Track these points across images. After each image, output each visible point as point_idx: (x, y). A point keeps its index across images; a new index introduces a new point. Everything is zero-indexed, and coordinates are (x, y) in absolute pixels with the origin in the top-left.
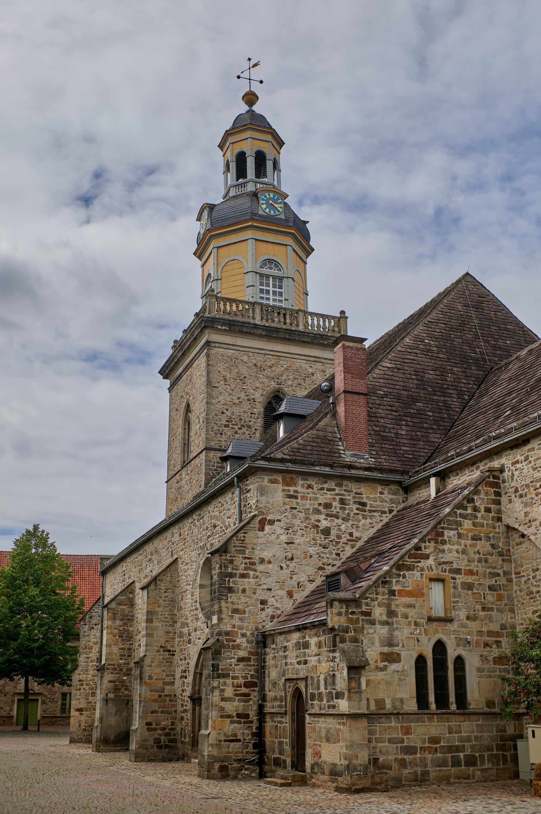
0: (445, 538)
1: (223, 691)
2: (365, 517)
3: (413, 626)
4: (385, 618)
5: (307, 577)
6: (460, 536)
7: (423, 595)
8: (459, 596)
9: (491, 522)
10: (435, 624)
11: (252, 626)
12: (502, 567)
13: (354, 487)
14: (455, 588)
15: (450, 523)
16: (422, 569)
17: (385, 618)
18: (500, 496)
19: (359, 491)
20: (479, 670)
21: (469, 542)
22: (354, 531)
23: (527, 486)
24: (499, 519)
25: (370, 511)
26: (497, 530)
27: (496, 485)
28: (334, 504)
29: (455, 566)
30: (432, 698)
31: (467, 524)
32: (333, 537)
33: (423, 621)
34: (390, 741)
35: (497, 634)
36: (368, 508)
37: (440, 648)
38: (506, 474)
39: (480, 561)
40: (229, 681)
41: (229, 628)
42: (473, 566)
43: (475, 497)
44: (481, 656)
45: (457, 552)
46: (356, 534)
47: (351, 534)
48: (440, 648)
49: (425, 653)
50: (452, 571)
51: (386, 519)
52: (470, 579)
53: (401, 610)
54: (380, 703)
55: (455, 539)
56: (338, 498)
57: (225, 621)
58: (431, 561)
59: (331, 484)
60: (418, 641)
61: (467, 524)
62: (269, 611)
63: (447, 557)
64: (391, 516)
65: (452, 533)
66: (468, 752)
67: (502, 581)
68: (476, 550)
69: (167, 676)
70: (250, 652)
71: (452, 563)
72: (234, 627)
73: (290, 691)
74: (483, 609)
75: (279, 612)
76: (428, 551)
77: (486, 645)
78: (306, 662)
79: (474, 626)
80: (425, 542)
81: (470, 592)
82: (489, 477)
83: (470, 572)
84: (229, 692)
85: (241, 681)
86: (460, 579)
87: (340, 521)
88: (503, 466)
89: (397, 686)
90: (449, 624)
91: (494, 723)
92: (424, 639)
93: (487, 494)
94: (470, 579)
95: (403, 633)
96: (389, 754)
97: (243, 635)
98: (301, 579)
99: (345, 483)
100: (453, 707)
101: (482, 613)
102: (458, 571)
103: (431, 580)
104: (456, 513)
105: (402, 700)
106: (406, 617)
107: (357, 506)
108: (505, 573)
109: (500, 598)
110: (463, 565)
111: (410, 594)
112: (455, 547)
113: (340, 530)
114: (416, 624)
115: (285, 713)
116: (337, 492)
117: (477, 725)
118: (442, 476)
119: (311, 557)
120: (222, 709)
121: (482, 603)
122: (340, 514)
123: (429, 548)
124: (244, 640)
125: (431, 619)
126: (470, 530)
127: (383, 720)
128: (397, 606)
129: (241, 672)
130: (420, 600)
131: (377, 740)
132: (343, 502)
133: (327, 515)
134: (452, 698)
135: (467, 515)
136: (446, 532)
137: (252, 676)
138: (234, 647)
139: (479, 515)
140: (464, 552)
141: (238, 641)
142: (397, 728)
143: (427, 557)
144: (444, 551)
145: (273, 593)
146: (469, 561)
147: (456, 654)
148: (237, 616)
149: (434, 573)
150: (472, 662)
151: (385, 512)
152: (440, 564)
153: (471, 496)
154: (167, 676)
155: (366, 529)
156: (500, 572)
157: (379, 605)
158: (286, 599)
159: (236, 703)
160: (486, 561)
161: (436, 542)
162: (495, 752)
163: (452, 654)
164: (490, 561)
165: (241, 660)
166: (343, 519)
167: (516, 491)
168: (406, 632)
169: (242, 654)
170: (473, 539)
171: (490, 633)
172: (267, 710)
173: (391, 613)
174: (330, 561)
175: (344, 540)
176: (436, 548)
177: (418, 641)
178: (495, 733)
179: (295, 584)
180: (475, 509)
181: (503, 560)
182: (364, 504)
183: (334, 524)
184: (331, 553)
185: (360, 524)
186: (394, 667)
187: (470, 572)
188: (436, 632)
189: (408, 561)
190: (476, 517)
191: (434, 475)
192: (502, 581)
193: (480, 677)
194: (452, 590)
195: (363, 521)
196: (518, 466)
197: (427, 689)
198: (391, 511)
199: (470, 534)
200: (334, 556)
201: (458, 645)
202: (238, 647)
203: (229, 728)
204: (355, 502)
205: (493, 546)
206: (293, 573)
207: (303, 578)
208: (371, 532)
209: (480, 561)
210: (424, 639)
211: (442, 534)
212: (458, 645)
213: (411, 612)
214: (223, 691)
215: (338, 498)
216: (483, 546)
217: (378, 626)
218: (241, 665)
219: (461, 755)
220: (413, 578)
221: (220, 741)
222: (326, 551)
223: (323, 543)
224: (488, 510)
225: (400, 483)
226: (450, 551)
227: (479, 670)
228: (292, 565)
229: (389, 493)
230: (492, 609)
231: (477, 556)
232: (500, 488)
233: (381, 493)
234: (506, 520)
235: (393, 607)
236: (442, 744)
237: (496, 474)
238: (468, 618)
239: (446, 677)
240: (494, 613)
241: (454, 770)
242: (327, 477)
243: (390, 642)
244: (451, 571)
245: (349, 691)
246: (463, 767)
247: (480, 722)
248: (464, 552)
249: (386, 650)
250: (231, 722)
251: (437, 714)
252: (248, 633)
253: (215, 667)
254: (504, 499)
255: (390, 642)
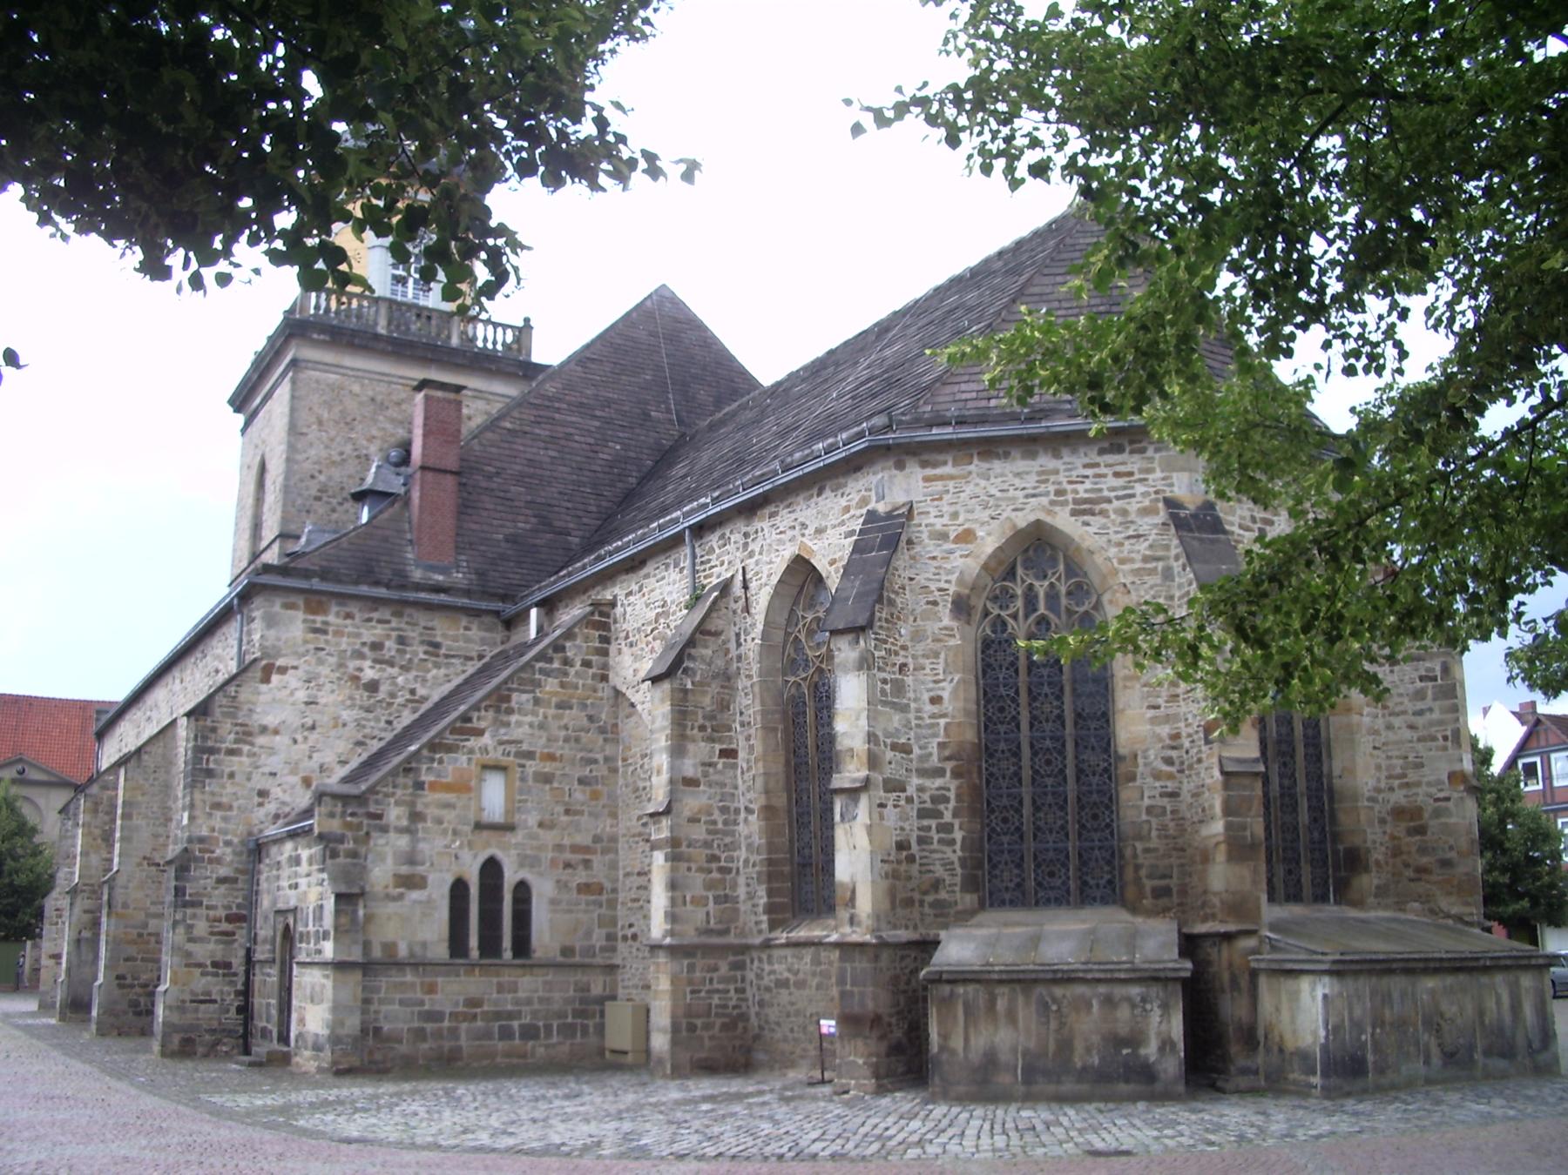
0: (513, 704)
1: (191, 927)
2: (437, 666)
3: (450, 837)
4: (405, 823)
5: (334, 757)
6: (537, 702)
7: (468, 789)
8: (529, 792)
9: (589, 681)
10: (485, 834)
11: (241, 829)
12: (603, 750)
13: (423, 619)
14: (523, 779)
15: (522, 682)
16: (471, 751)
17: (405, 823)
18: (609, 643)
19: (430, 624)
20: (553, 902)
21: (552, 711)
22: (417, 686)
23: (639, 630)
24: (604, 678)
25: (447, 656)
26: (600, 694)
27: (605, 626)
28: (387, 644)
29: (525, 747)
30: (474, 942)
31: (551, 685)
32: (381, 695)
33: (468, 829)
34: (401, 1002)
35: (586, 849)
36: (443, 651)
37: (491, 869)
38: (619, 610)
39: (566, 740)
40: (202, 912)
41: (205, 832)
42: (559, 749)
43: (568, 644)
44: (558, 882)
45: (531, 725)
46: (421, 691)
47: (413, 692)
48: (491, 869)
49: (467, 877)
50: (519, 754)
51: (471, 668)
52: (548, 767)
53: (432, 812)
54: (390, 948)
55: (530, 706)
56: (394, 634)
57: (200, 821)
58: (487, 739)
59: (385, 613)
60: (457, 857)
61: (551, 685)
62: (271, 807)
63: (517, 733)
64: (479, 664)
65: (525, 697)
66: (527, 1020)
67: (601, 770)
68: (562, 723)
69: (153, 903)
70: (237, 870)
71: (521, 742)
72: (213, 830)
73: (280, 927)
74: (567, 812)
75: (287, 809)
76: (483, 724)
77: (568, 865)
78: (296, 886)
79: (549, 837)
80: (479, 710)
81: (547, 787)
82: (592, 613)
83: (551, 757)
84: (201, 927)
85: (222, 913)
86: (532, 766)
87: (395, 671)
88: (615, 597)
89: (421, 923)
90: (509, 835)
91: (572, 979)
92: (466, 855)
93: (587, 639)
94: (548, 767)
95: (432, 845)
96: (395, 1016)
97: (228, 843)
98: (327, 760)
99: (408, 611)
100: (508, 955)
101: (564, 819)
102: (530, 755)
103: (485, 767)
104: (533, 667)
105: (424, 945)
106: (439, 821)
107: (425, 648)
108: (606, 759)
109: (595, 796)
110: (539, 744)
111: (449, 788)
112: (529, 719)
113: (395, 684)
114: (455, 833)
115: (274, 961)
116: (394, 624)
117: (546, 983)
118: (549, 606)
119: (344, 725)
120: (189, 954)
121: (566, 804)
122: (397, 659)
123: (484, 720)
124: (229, 850)
125: (479, 826)
126: (556, 694)
127: (393, 972)
128: (426, 805)
129: (220, 899)
130: (465, 796)
131: (381, 1002)
132: (402, 641)
133: (376, 661)
134: (507, 942)
135: (552, 670)
136: (515, 696)
137: (239, 906)
138: (211, 861)
139: (572, 671)
140: (541, 726)
141: (218, 852)
142: (413, 985)
143: (480, 733)
144: (508, 724)
145: (278, 780)
146: (549, 740)
147: (518, 877)
148: (218, 814)
149: (496, 755)
150: (543, 890)
151: (471, 659)
152: (501, 743)
153: (561, 642)
154: (153, 903)
155: (437, 684)
156: (600, 757)
157: (397, 803)
158: (300, 789)
159: (211, 946)
160: (577, 740)
161: (498, 710)
162: (570, 1020)
163: (510, 877)
164: (584, 740)
165: (222, 881)
166: (402, 667)
167: (627, 637)
168: (440, 842)
169: (223, 871)
170: (560, 706)
171: (575, 849)
172: (258, 956)
173: (416, 817)
174: (376, 732)
175: (400, 700)
176: (495, 720)
177: (457, 857)
178: (571, 993)
179: (316, 767)
180: (567, 662)
181: (605, 740)
182: (437, 646)
183: (385, 675)
184: (377, 720)
185: (429, 676)
186: (415, 895)
187: (551, 757)
188: (488, 845)
189: (450, 739)
190: (566, 674)
191: (537, 605)
192: (601, 770)
193: (555, 911)
194: (518, 783)
195: (434, 671)
196: (632, 599)
197: (468, 929)
198: (481, 657)
199: (554, 700)
200: (382, 724)
201: (521, 865)
202: (218, 861)
203: (200, 983)
204: (422, 642)
205: (591, 718)
206: (313, 749)
207: (328, 757)
208: (447, 688)
209: (566, 740)
210: (466, 855)
211: (508, 699)
212: (521, 865)
213: (449, 816)
214: (191, 927)
215: (394, 634)
216: (574, 717)
217: (392, 835)
218: (223, 888)
219: (516, 1024)
220: (455, 765)
221: (183, 1001)
222: (371, 716)
223: (366, 703)
224: (587, 664)
225: (497, 613)
226: (519, 724)
227: (553, 902)
228: (313, 737)
229: (479, 629)
230: (581, 813)
231: (563, 733)
232: (609, 630)
233: (467, 628)
234: (615, 680)
235: (419, 808)
236: (486, 1008)
237: (605, 609)
238: (541, 825)
239: (499, 912)
240: (585, 819)
241: (501, 1045)
242: (377, 602)
243: (411, 859)
244: (519, 754)
245: (336, 929)
246: (517, 1041)
247: (549, 978)
248: (541, 726)
249: (404, 870)
250: (203, 974)
251: (481, 965)
252: (236, 840)
253: (179, 891)
254: (613, 648)
255: (411, 859)
